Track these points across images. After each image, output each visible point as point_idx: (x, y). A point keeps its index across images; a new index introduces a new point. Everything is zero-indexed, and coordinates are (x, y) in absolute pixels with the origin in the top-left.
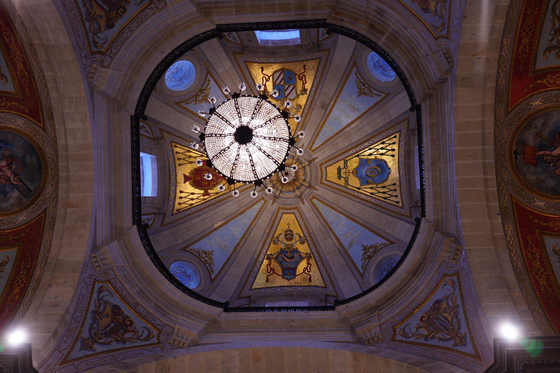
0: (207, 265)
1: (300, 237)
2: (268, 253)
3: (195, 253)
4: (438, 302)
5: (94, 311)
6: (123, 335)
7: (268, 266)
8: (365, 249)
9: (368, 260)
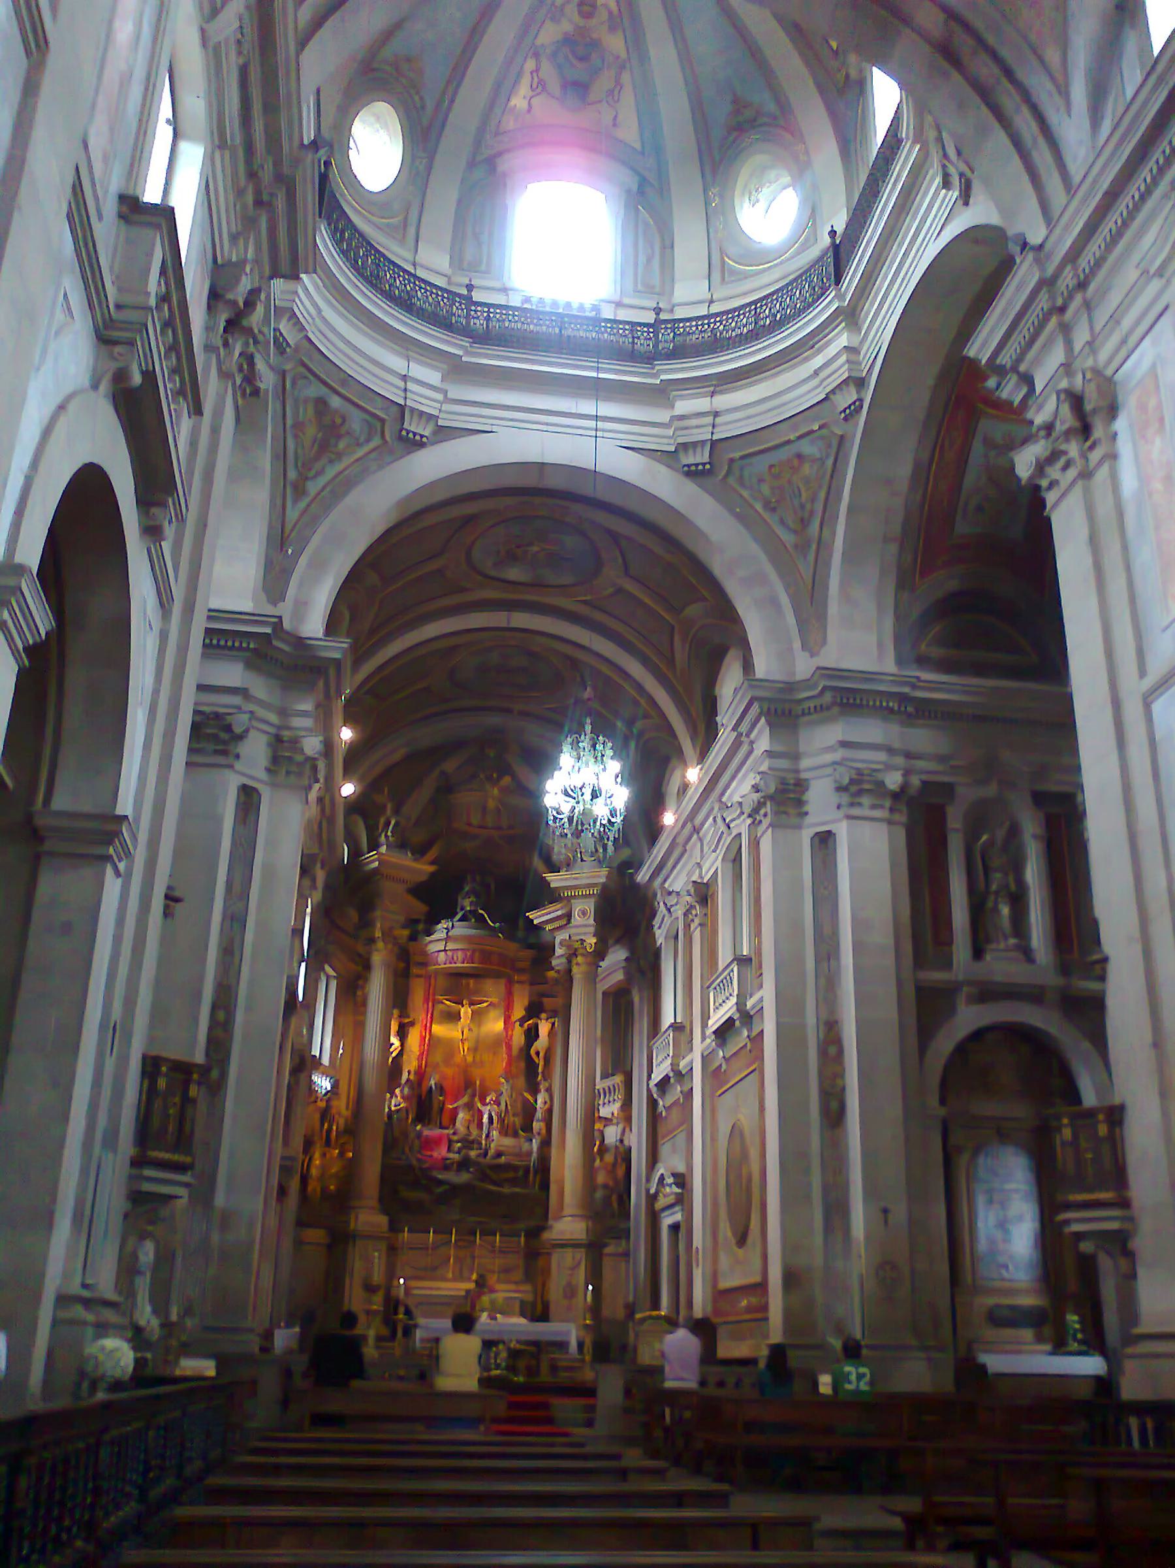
0: (412, 92)
1: (610, 12)
2: (539, 42)
3: (388, 68)
4: (799, 456)
5: (294, 426)
6: (336, 445)
7: (535, 74)
8: (739, 105)
9: (735, 134)
